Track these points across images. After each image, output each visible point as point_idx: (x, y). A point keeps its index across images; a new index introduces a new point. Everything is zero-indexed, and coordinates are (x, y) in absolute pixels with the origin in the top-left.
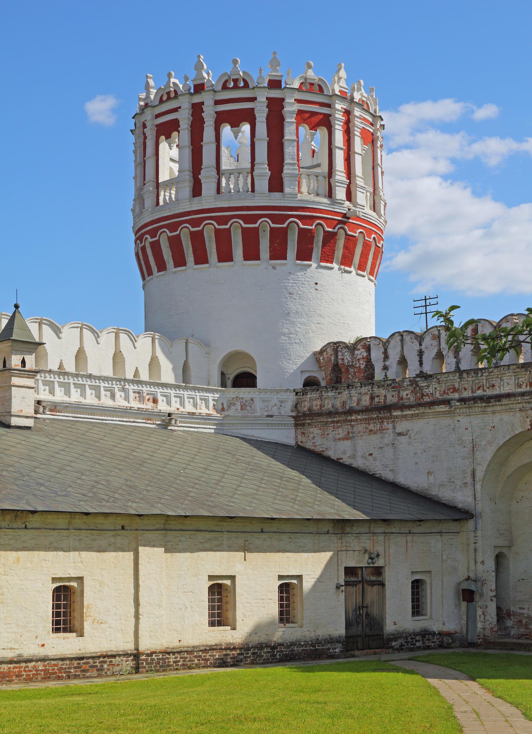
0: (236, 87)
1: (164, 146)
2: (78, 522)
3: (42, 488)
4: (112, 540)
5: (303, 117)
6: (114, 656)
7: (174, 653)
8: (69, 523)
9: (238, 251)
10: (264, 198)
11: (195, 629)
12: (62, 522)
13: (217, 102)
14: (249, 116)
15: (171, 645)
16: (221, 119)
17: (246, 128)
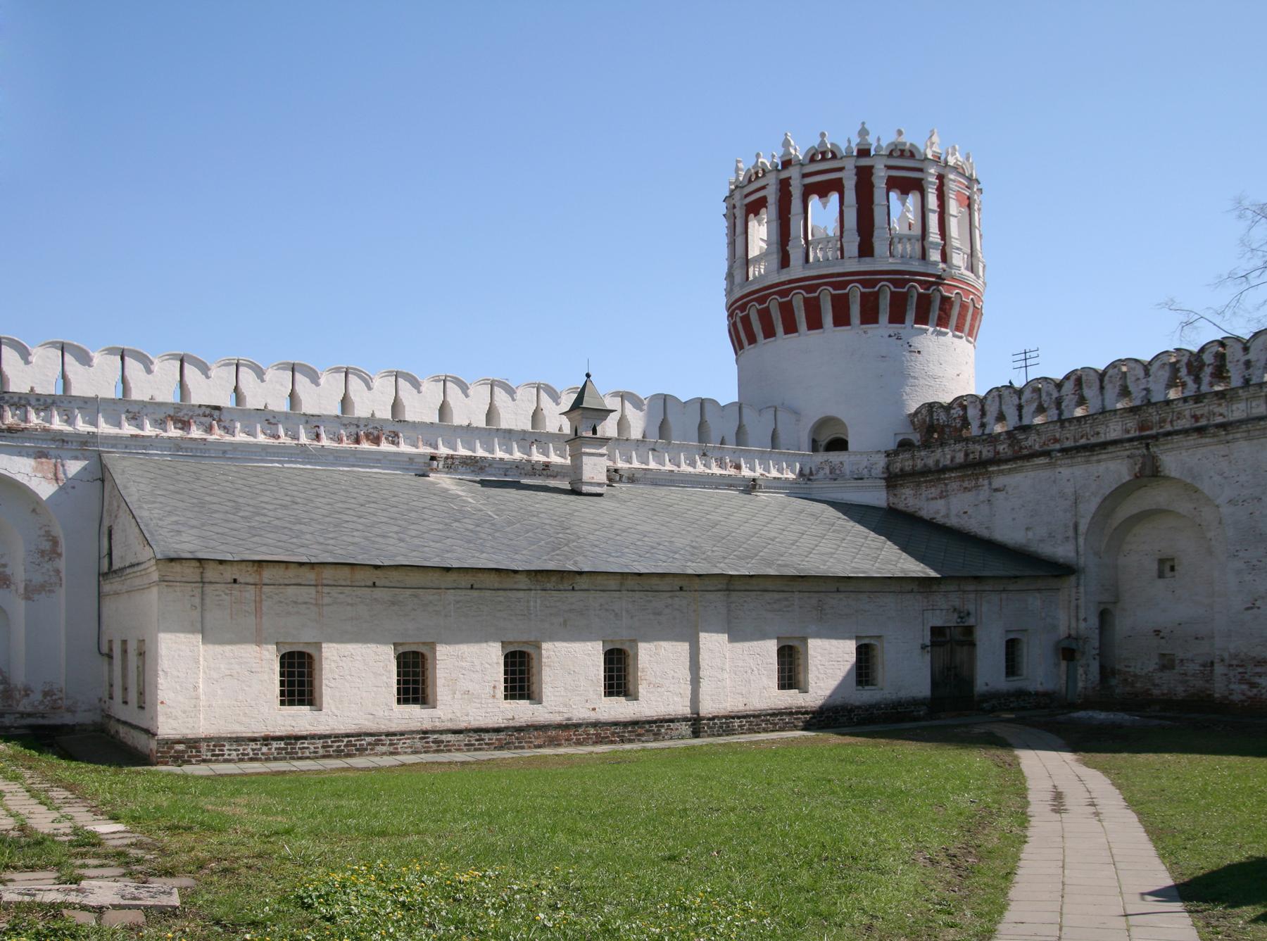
0: (824, 159)
1: (753, 224)
2: (630, 583)
3: (596, 550)
4: (670, 601)
5: (892, 183)
6: (672, 721)
7: (739, 717)
8: (621, 584)
9: (828, 318)
10: (853, 265)
11: (765, 692)
12: (613, 584)
13: (805, 176)
14: (837, 186)
15: (736, 709)
16: (808, 191)
17: (834, 198)
